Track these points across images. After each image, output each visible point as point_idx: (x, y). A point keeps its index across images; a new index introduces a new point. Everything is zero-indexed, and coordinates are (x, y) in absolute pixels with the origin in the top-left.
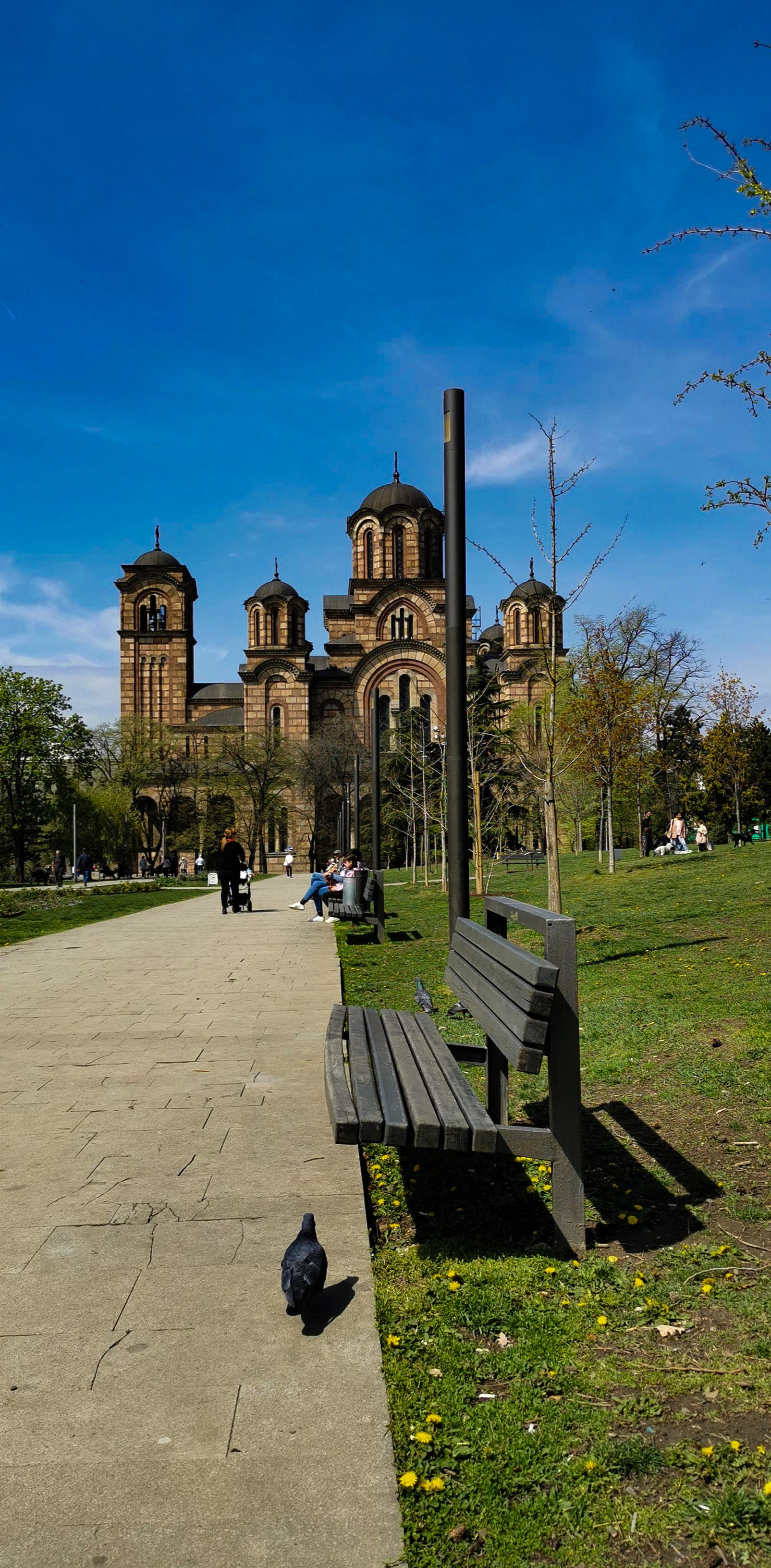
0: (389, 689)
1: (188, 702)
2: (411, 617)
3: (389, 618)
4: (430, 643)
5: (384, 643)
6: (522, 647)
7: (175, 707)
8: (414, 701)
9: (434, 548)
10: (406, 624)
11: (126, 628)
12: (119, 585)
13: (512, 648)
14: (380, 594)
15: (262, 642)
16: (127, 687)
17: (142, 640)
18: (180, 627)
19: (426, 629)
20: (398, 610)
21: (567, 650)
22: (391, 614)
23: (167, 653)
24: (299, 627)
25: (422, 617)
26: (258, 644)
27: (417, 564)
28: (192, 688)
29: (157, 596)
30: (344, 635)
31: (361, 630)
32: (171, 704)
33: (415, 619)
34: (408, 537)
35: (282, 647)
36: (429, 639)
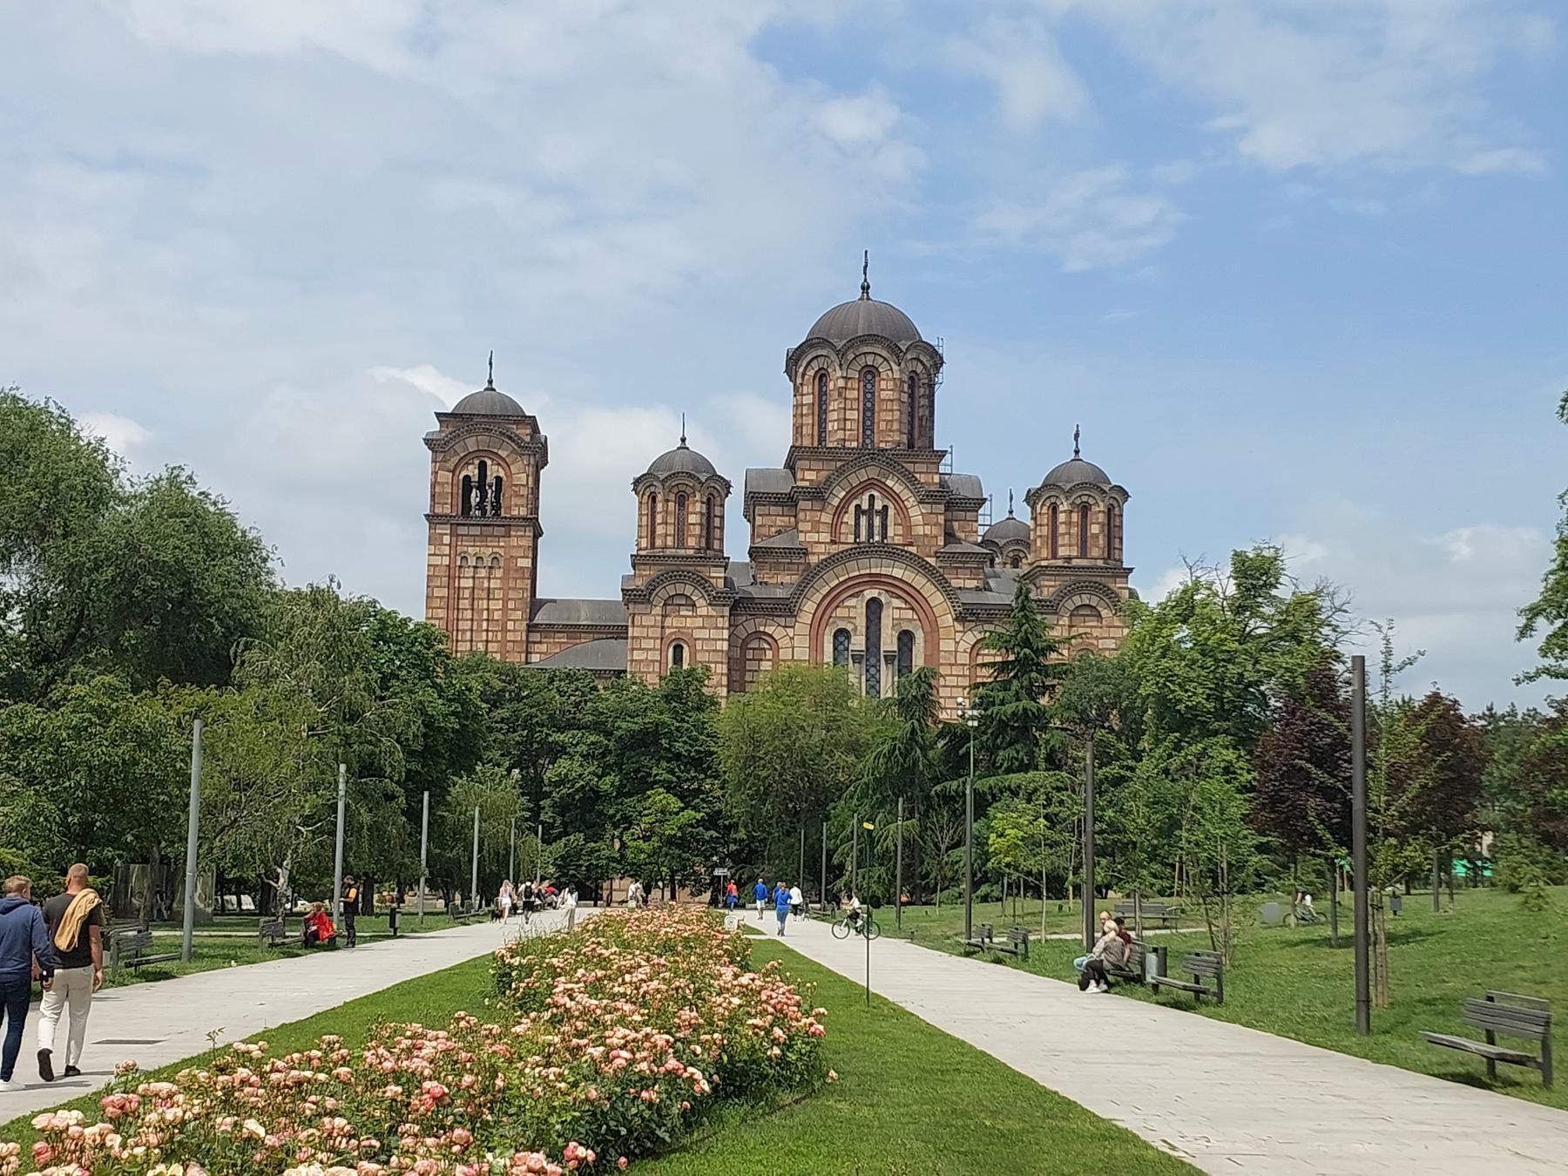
1: (531, 628)
2: (885, 508)
3: (852, 508)
4: (913, 549)
5: (842, 547)
6: (1060, 563)
7: (510, 636)
8: (889, 643)
9: (923, 401)
10: (877, 521)
11: (438, 510)
12: (428, 442)
13: (1044, 563)
14: (840, 471)
15: (658, 542)
16: (437, 603)
17: (462, 530)
18: (523, 512)
19: (909, 528)
20: (866, 497)
21: (1131, 570)
22: (855, 502)
23: (501, 551)
24: (717, 521)
25: (902, 510)
26: (653, 546)
27: (896, 426)
28: (535, 605)
29: (489, 462)
30: (779, 532)
31: (808, 526)
32: (505, 630)
33: (891, 512)
34: (883, 385)
35: (691, 552)
36: (911, 544)
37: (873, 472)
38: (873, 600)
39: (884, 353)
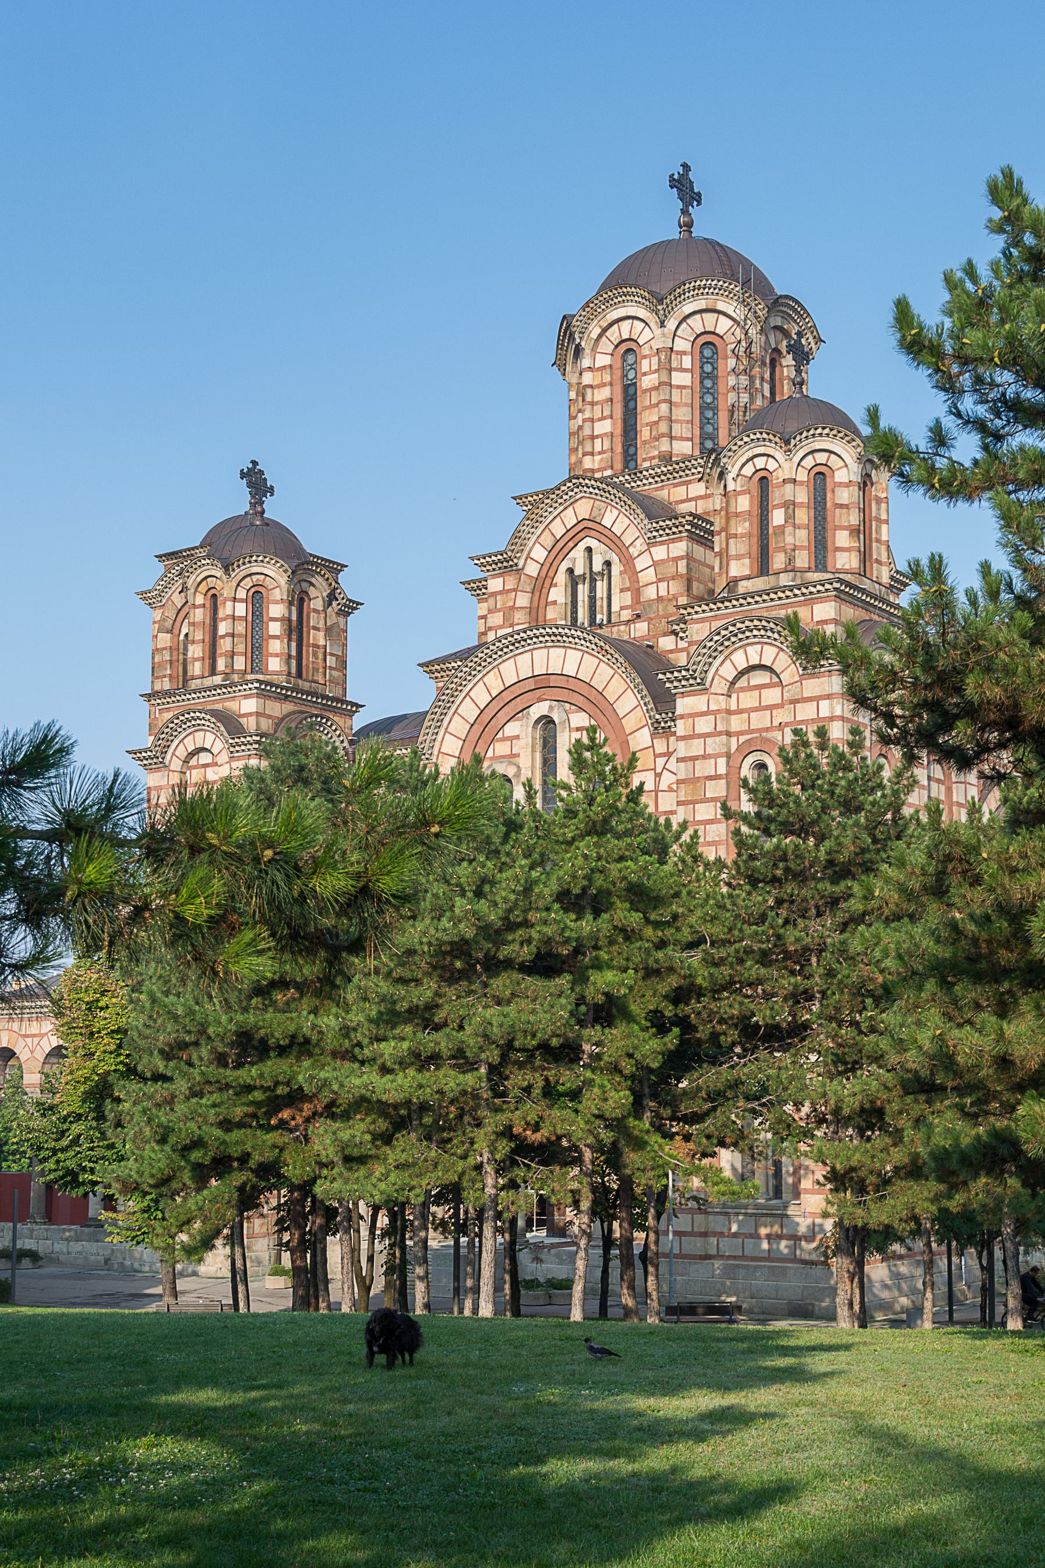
0: (512, 757)
2: (608, 564)
9: (732, 381)
11: (157, 688)
19: (636, 591)
20: (578, 554)
25: (628, 562)
33: (616, 569)
34: (645, 365)
35: (218, 680)
37: (583, 508)
38: (547, 721)
39: (642, 313)
